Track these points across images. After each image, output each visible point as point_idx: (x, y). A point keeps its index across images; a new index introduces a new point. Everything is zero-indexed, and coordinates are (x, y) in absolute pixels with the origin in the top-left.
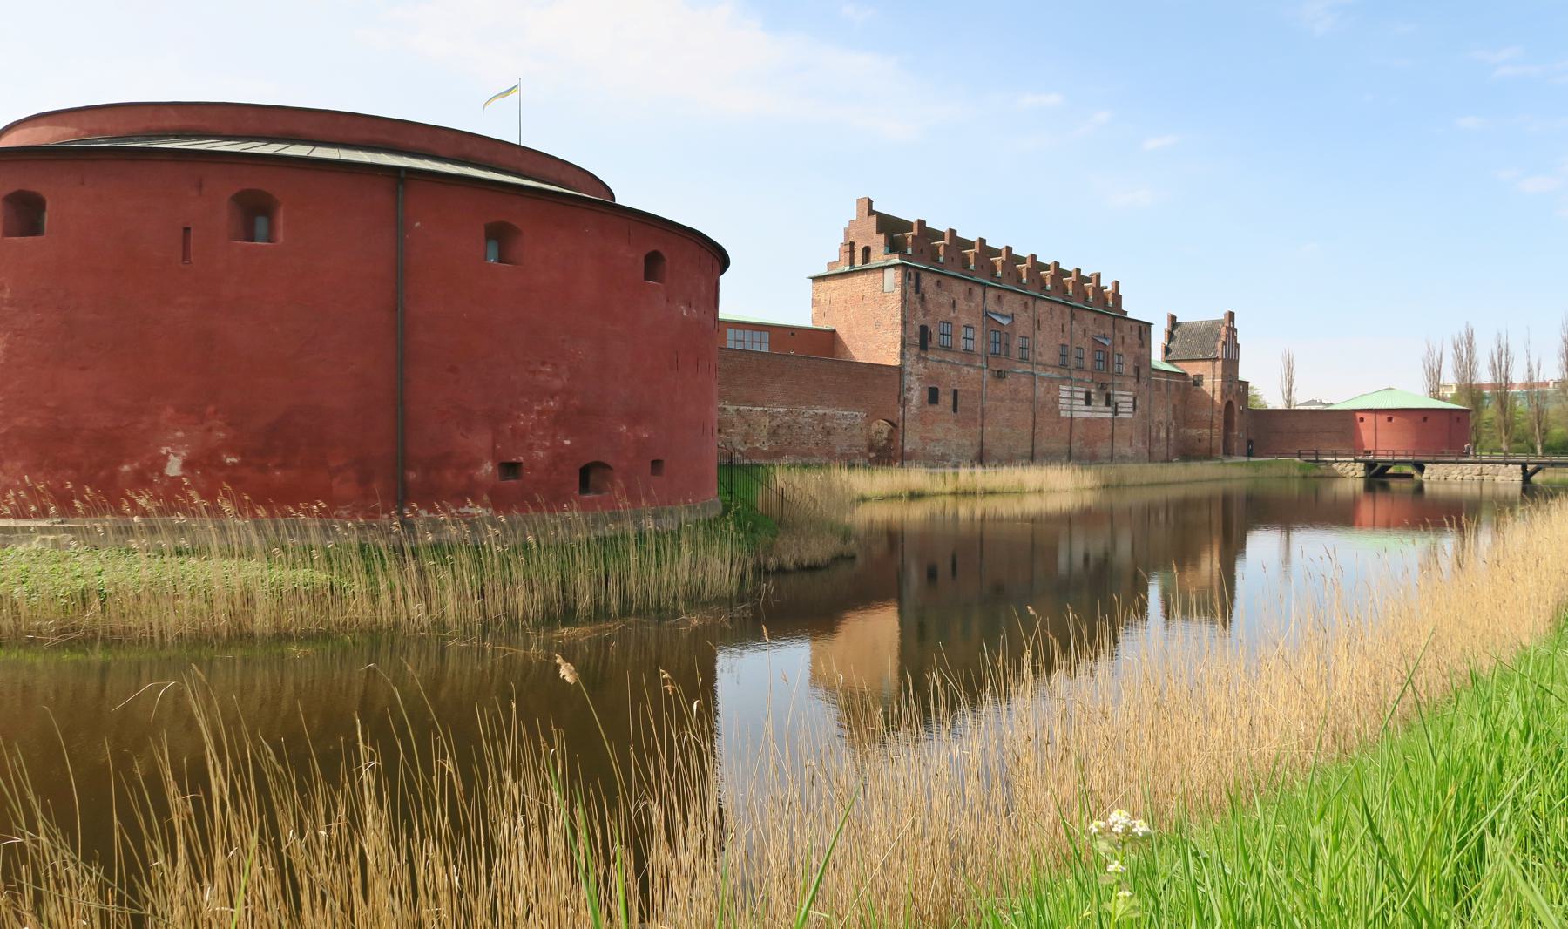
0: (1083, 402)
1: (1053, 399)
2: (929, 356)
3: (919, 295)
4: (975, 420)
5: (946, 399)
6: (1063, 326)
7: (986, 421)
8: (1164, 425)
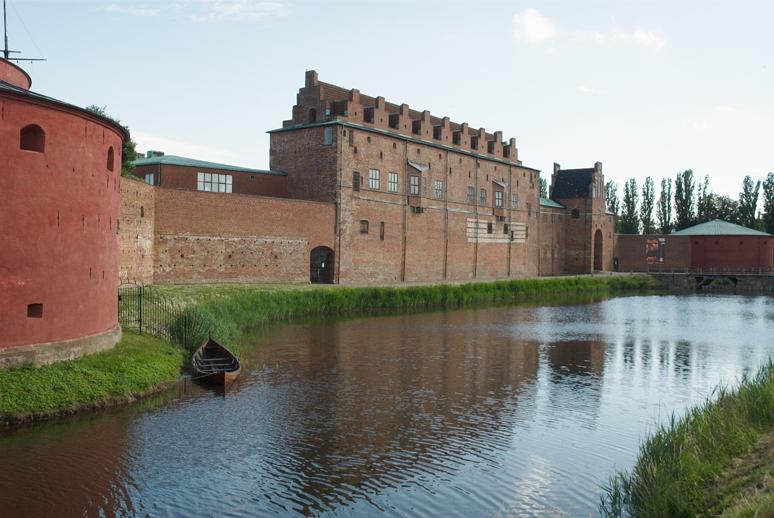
0: (486, 231)
4: (398, 245)
5: (375, 230)
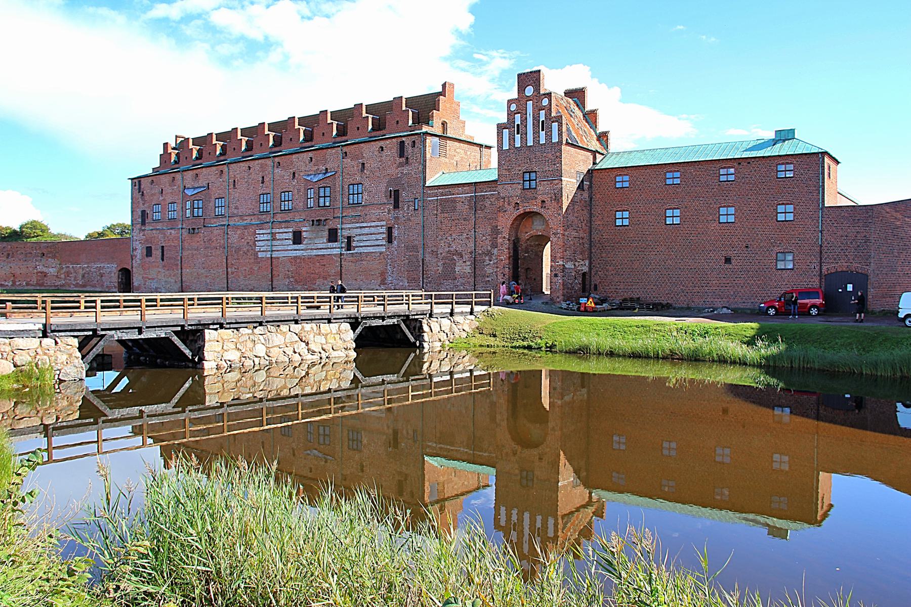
0: (291, 242)
1: (248, 243)
2: (147, 229)
3: (141, 193)
4: (178, 264)
5: (157, 253)
6: (263, 177)
7: (184, 265)
8: (466, 257)
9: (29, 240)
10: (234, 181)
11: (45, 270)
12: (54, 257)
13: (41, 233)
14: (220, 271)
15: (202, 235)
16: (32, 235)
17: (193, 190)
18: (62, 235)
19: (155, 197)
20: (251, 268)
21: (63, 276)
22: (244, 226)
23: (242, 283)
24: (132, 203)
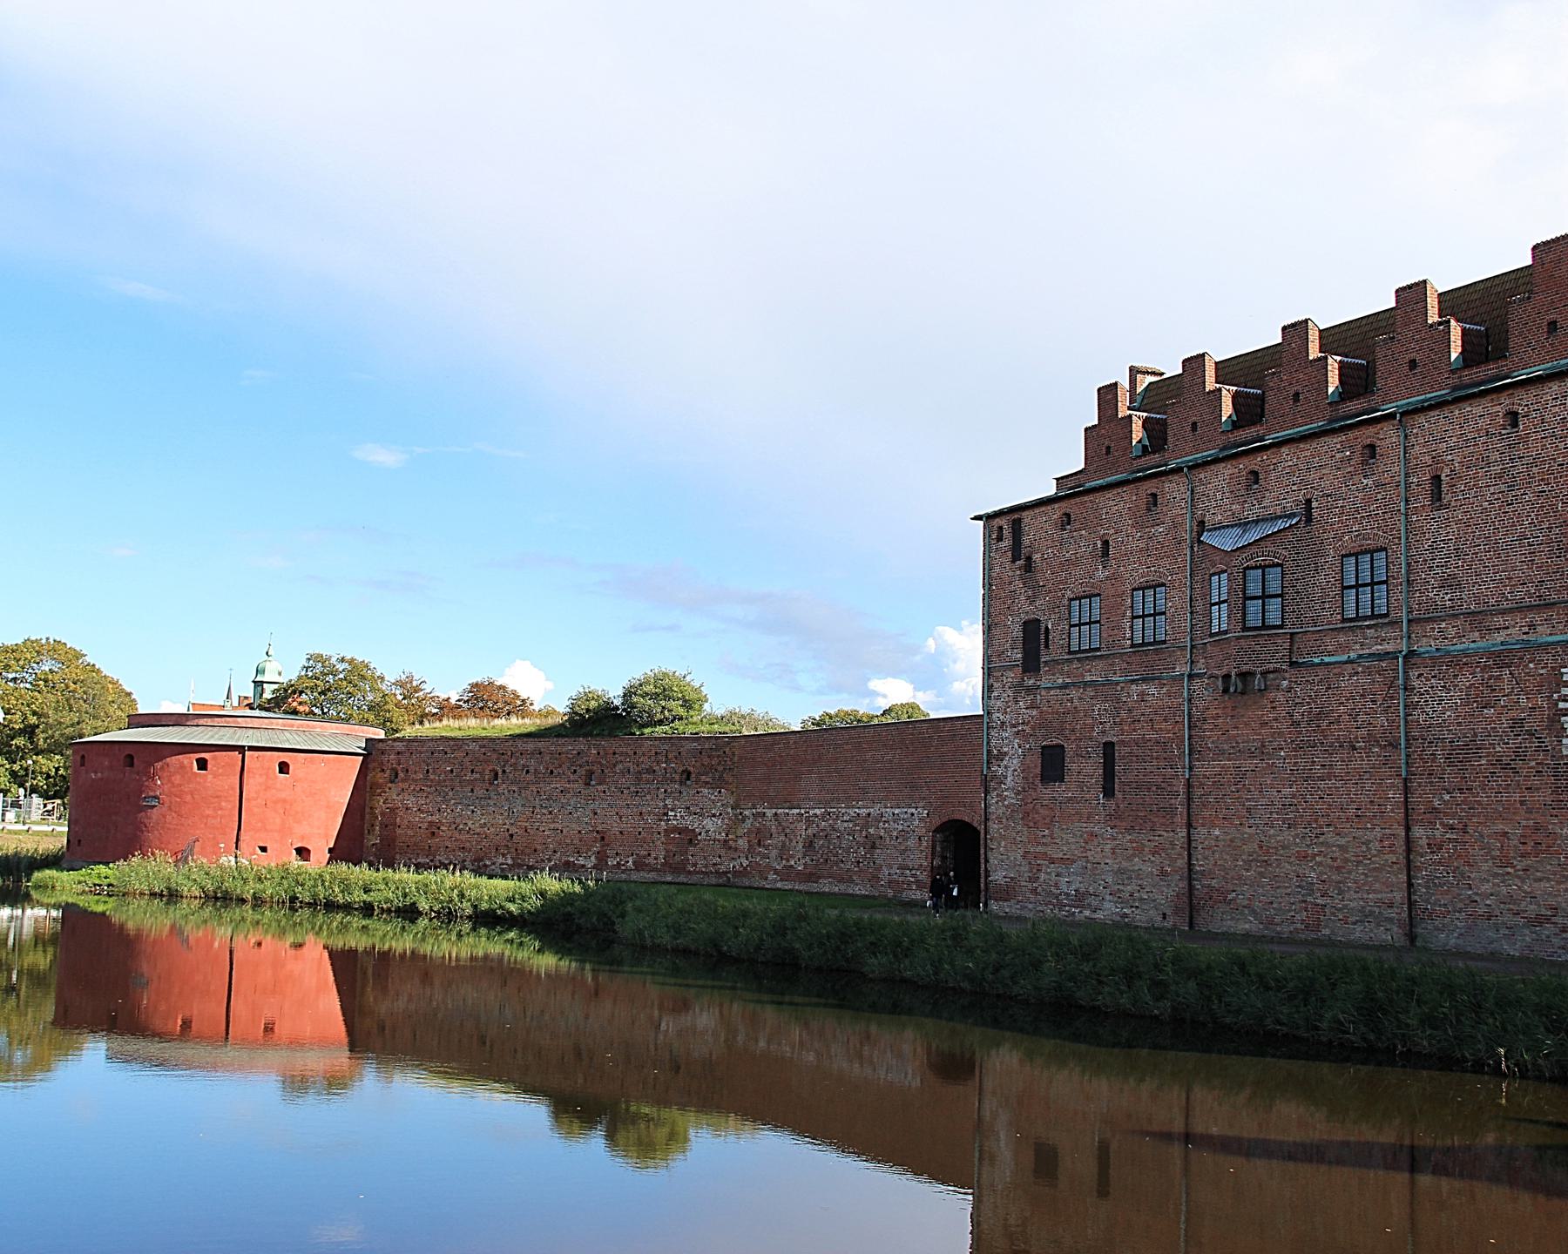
1: (1517, 723)
4: (1171, 811)
5: (1084, 769)
9: (647, 731)
10: (1436, 479)
11: (691, 822)
12: (718, 784)
13: (681, 711)
14: (1369, 835)
15: (1280, 697)
16: (659, 716)
17: (1239, 531)
18: (743, 717)
19: (1076, 572)
20: (1537, 828)
21: (742, 843)
22: (1491, 655)
23: (1487, 888)
24: (989, 598)
